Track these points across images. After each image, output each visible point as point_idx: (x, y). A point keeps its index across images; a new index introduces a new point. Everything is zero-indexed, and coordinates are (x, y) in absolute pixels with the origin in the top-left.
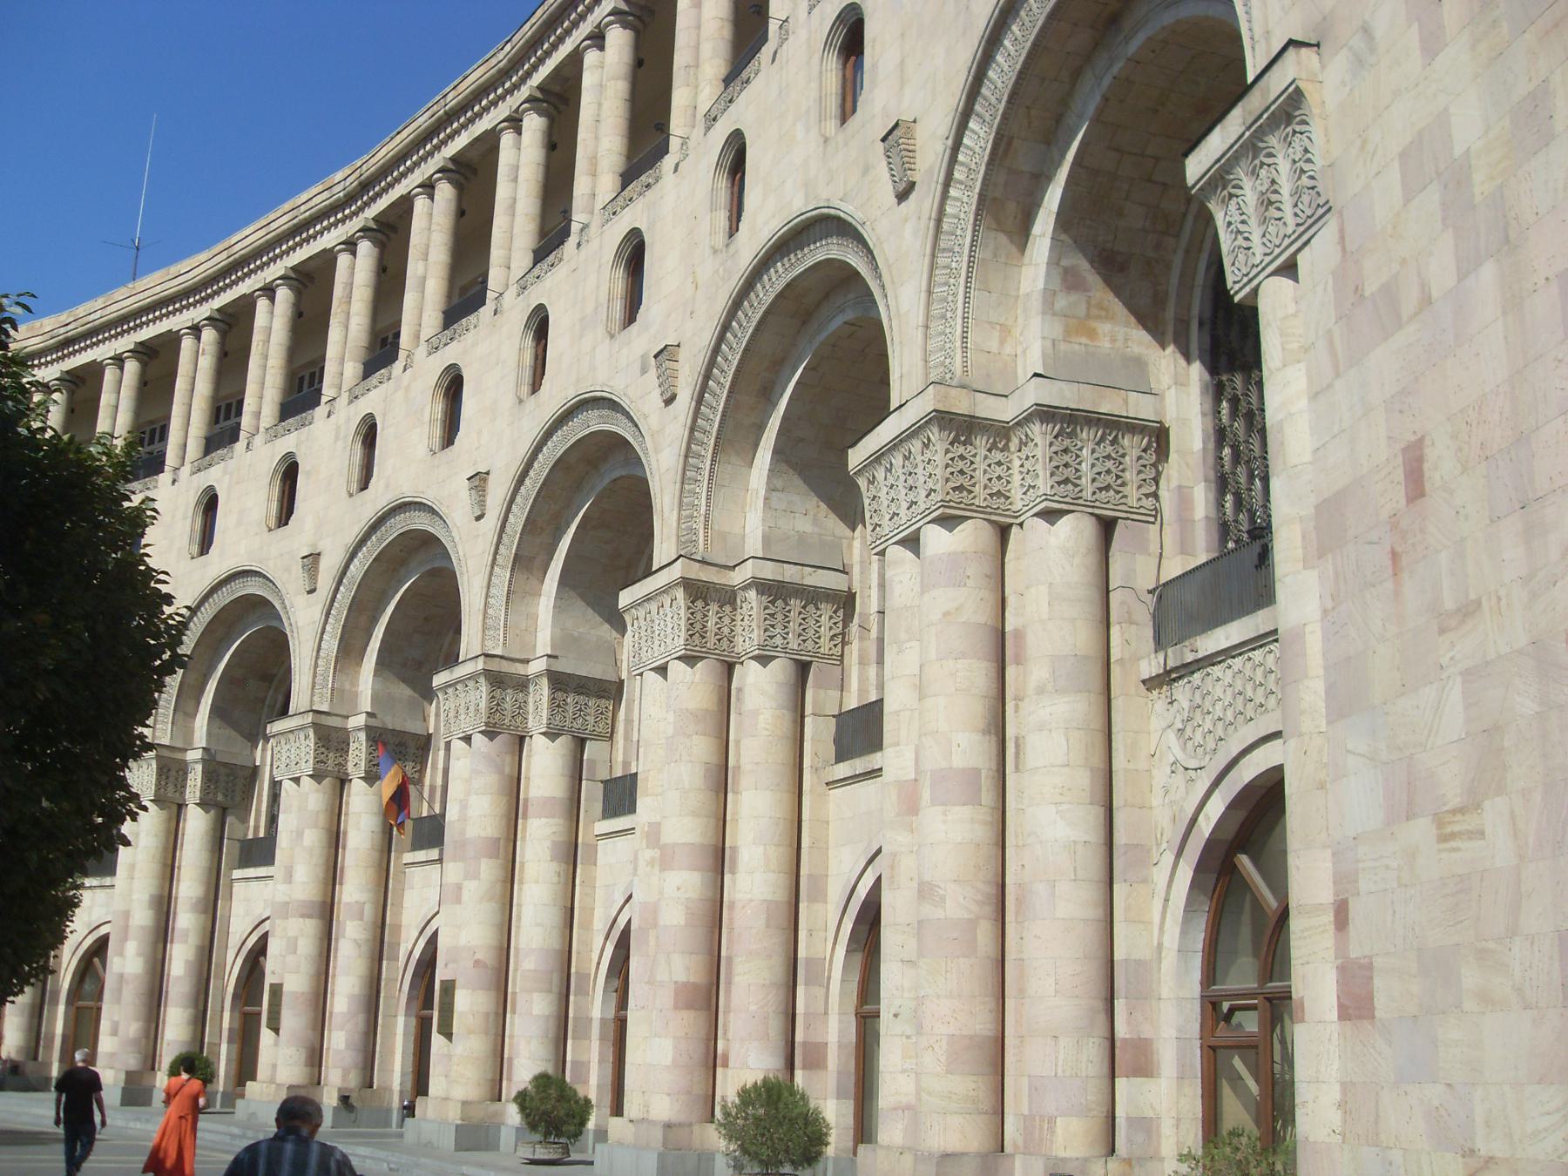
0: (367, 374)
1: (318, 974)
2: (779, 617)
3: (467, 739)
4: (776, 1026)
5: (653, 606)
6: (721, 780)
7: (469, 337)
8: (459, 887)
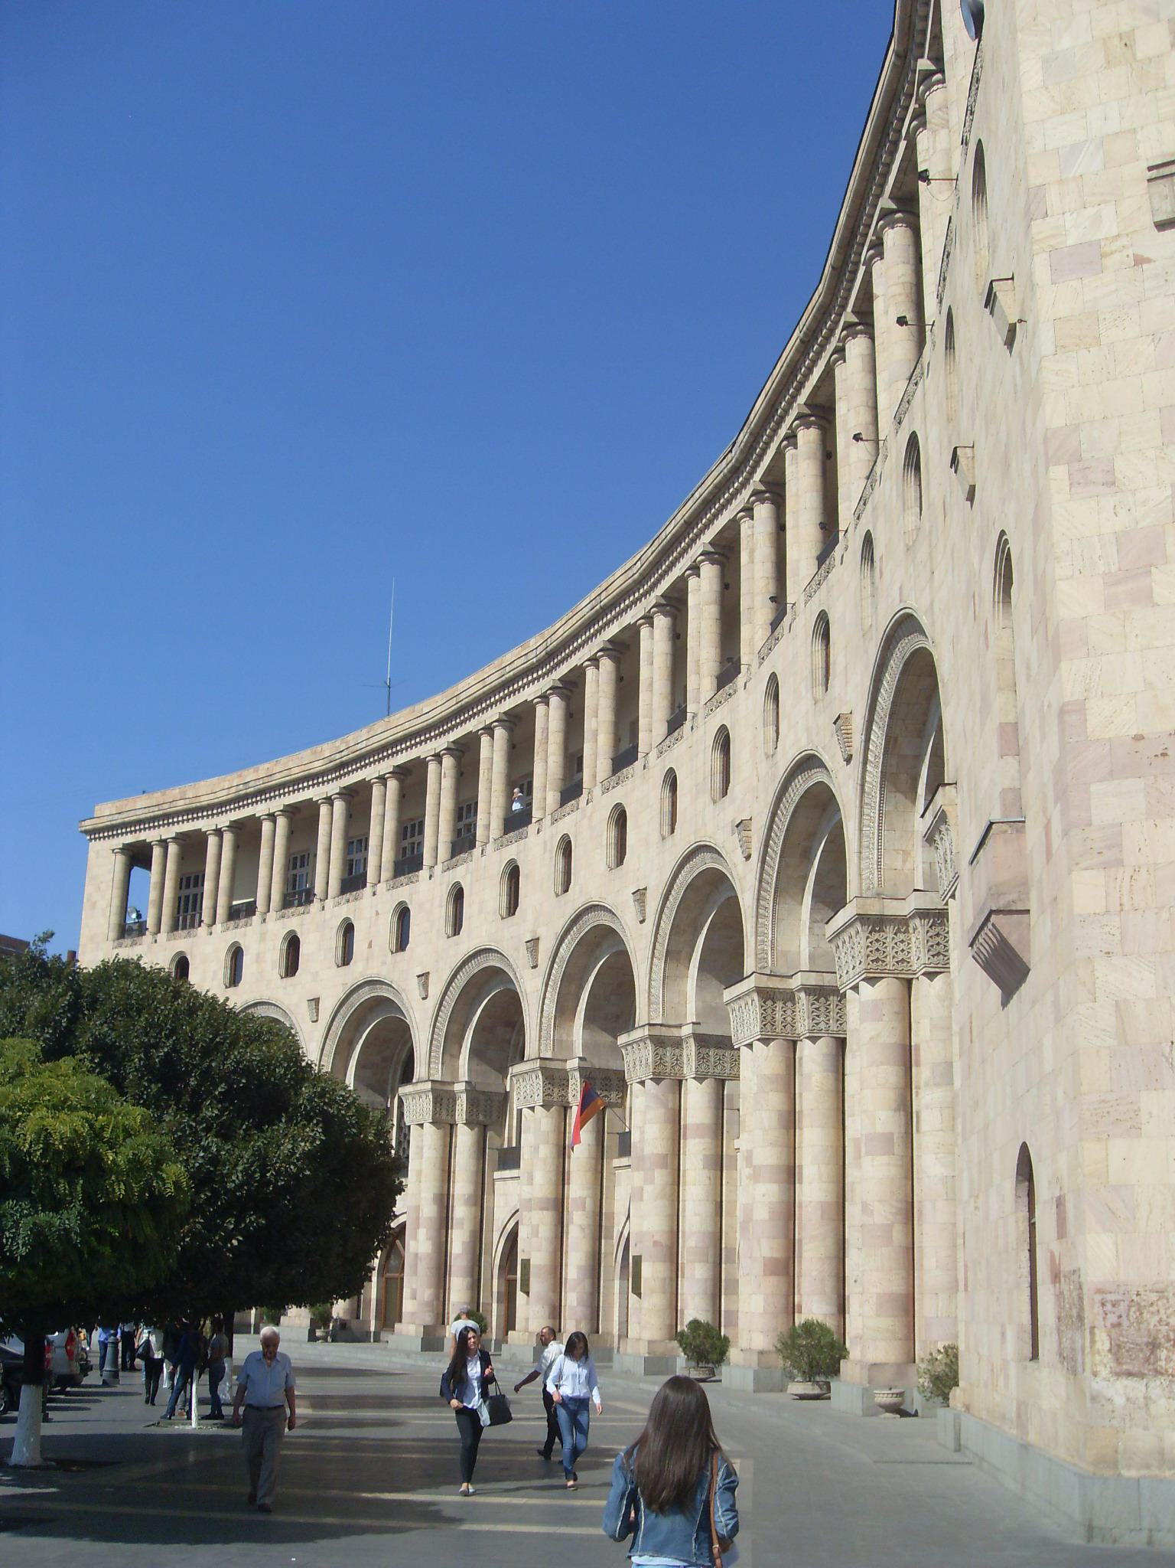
1: (555, 1252)
2: (823, 1009)
3: (642, 1083)
4: (830, 1285)
5: (742, 1003)
6: (790, 1120)
7: (629, 782)
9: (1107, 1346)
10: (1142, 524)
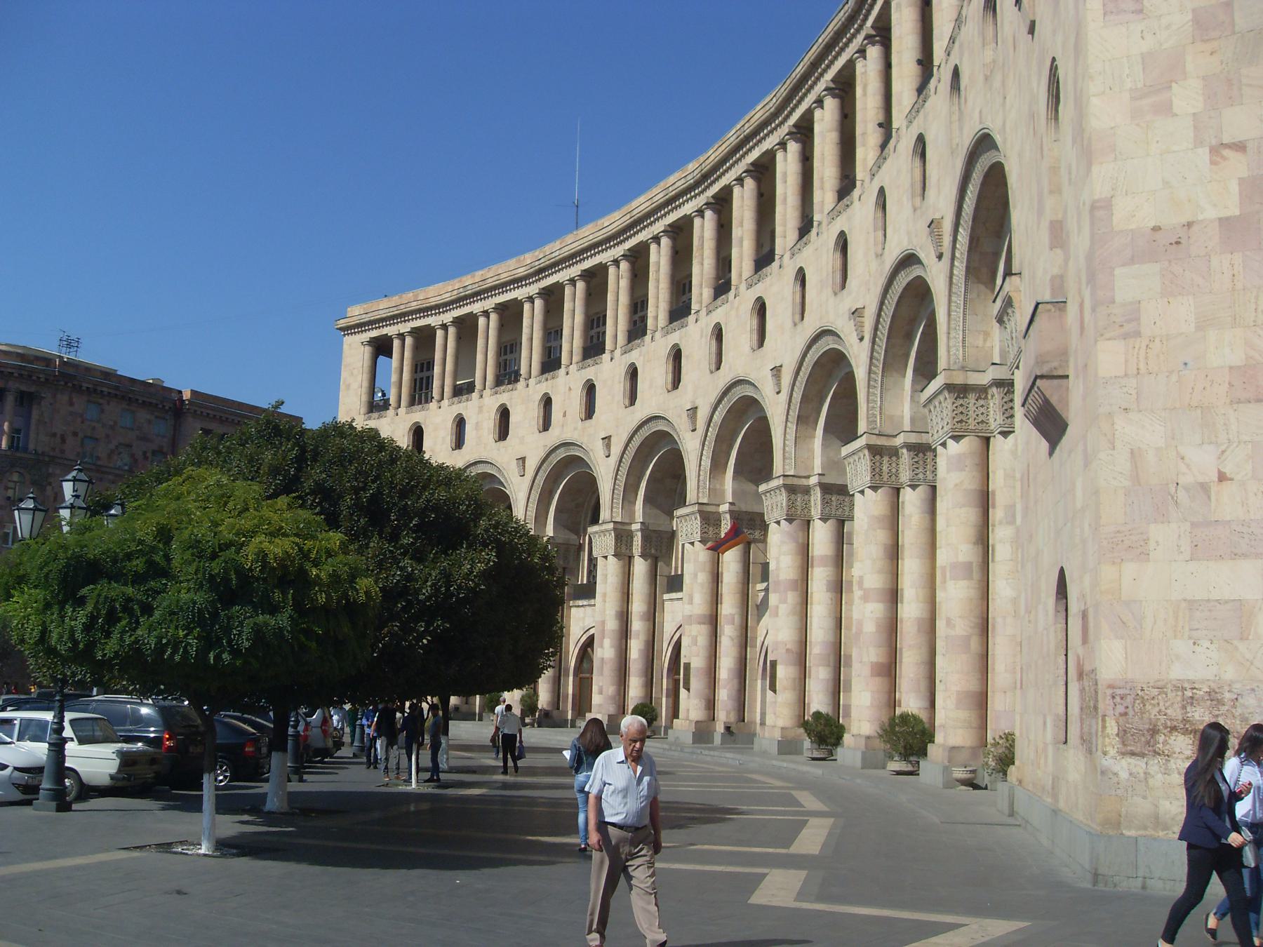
0: (716, 296)
3: (778, 523)
4: (924, 685)
5: (856, 457)
6: (894, 553)
8: (777, 607)
9: (1115, 731)
10: (1165, 46)
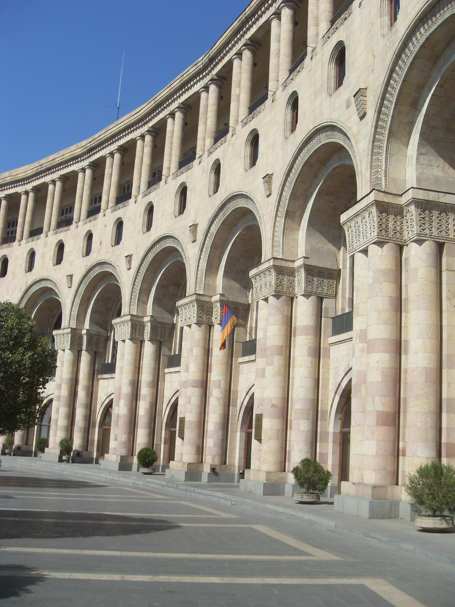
0: (215, 142)
1: (200, 413)
2: (427, 219)
3: (266, 300)
4: (431, 434)
5: (359, 219)
6: (398, 305)
7: (261, 115)
8: (264, 370)
